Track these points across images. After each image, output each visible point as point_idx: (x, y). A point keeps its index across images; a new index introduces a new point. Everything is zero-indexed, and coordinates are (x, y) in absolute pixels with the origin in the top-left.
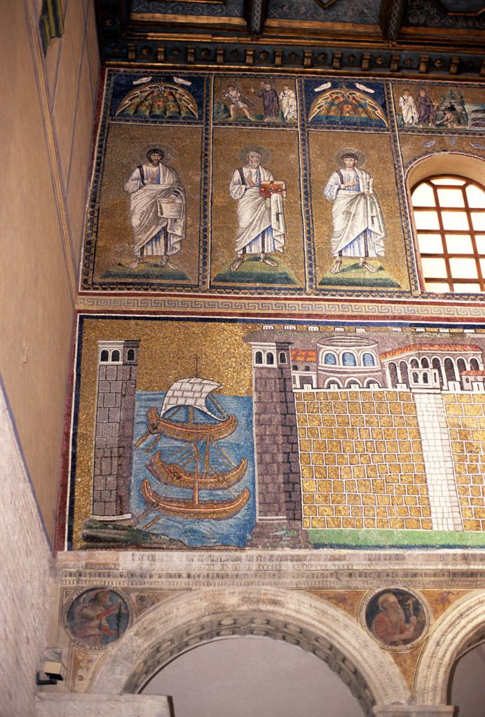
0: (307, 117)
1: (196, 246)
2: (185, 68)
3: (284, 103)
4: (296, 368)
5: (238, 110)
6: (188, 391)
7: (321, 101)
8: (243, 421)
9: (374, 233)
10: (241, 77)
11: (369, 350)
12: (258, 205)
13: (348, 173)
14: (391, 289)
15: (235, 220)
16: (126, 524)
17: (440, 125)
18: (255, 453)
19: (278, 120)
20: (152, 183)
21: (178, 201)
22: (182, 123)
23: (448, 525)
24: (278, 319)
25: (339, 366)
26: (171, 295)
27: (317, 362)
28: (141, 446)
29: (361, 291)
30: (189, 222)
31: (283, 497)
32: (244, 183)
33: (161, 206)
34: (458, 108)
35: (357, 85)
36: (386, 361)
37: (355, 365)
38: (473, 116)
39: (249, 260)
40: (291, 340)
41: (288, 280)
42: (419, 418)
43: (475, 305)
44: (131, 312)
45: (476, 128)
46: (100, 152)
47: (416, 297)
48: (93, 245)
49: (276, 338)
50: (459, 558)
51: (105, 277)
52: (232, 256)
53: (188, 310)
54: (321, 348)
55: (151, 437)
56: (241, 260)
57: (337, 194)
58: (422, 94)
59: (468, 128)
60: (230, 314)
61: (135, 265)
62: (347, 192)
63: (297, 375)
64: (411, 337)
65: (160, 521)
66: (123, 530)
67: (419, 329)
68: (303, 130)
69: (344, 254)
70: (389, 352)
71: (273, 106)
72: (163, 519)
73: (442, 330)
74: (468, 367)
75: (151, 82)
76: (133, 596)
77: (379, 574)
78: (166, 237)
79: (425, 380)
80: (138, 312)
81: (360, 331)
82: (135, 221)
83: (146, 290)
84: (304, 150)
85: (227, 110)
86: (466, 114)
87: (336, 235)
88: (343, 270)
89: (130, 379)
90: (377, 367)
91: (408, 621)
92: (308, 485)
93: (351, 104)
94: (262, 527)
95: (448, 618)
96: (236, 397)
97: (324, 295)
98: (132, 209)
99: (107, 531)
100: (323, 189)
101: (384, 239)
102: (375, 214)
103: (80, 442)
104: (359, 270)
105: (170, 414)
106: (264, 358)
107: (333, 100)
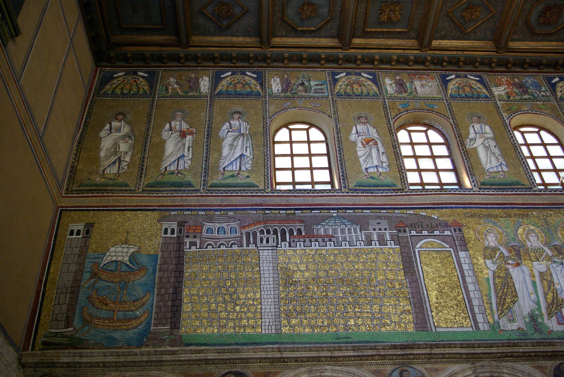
0: (214, 92)
1: (137, 167)
2: (144, 67)
3: (202, 84)
4: (188, 237)
5: (174, 89)
6: (119, 252)
7: (224, 82)
8: (151, 270)
9: (247, 156)
10: (178, 70)
11: (234, 225)
13: (235, 123)
14: (253, 189)
15: (163, 151)
16: (69, 334)
17: (294, 93)
19: (198, 94)
20: (116, 132)
21: (130, 142)
22: (139, 97)
23: (271, 329)
24: (180, 208)
25: (215, 235)
27: (201, 233)
28: (86, 286)
32: (171, 130)
34: (306, 84)
35: (247, 73)
36: (244, 231)
38: (315, 87)
39: (169, 174)
40: (187, 220)
41: (190, 185)
42: (261, 265)
43: (303, 196)
44: (92, 207)
45: (316, 95)
46: (87, 115)
47: (268, 193)
48: (75, 168)
50: (276, 350)
53: (127, 204)
54: (205, 225)
55: (92, 280)
56: (163, 174)
57: (227, 134)
58: (286, 76)
59: (311, 94)
60: (152, 206)
61: (98, 179)
62: (233, 134)
63: (187, 241)
65: (91, 332)
67: (267, 212)
68: (210, 99)
69: (226, 169)
71: (195, 86)
72: (93, 330)
74: (295, 234)
75: (124, 75)
78: (120, 163)
79: (267, 241)
80: (96, 207)
81: (230, 213)
82: (102, 154)
84: (210, 110)
85: (167, 89)
86: (311, 87)
87: (223, 158)
88: (225, 179)
89: (85, 246)
90: (238, 234)
92: (186, 307)
93: (242, 83)
94: (154, 333)
96: (149, 255)
97: (211, 193)
99: (57, 339)
100: (219, 132)
102: (248, 145)
104: (235, 178)
105: (105, 267)
106: (169, 231)
107: (231, 82)
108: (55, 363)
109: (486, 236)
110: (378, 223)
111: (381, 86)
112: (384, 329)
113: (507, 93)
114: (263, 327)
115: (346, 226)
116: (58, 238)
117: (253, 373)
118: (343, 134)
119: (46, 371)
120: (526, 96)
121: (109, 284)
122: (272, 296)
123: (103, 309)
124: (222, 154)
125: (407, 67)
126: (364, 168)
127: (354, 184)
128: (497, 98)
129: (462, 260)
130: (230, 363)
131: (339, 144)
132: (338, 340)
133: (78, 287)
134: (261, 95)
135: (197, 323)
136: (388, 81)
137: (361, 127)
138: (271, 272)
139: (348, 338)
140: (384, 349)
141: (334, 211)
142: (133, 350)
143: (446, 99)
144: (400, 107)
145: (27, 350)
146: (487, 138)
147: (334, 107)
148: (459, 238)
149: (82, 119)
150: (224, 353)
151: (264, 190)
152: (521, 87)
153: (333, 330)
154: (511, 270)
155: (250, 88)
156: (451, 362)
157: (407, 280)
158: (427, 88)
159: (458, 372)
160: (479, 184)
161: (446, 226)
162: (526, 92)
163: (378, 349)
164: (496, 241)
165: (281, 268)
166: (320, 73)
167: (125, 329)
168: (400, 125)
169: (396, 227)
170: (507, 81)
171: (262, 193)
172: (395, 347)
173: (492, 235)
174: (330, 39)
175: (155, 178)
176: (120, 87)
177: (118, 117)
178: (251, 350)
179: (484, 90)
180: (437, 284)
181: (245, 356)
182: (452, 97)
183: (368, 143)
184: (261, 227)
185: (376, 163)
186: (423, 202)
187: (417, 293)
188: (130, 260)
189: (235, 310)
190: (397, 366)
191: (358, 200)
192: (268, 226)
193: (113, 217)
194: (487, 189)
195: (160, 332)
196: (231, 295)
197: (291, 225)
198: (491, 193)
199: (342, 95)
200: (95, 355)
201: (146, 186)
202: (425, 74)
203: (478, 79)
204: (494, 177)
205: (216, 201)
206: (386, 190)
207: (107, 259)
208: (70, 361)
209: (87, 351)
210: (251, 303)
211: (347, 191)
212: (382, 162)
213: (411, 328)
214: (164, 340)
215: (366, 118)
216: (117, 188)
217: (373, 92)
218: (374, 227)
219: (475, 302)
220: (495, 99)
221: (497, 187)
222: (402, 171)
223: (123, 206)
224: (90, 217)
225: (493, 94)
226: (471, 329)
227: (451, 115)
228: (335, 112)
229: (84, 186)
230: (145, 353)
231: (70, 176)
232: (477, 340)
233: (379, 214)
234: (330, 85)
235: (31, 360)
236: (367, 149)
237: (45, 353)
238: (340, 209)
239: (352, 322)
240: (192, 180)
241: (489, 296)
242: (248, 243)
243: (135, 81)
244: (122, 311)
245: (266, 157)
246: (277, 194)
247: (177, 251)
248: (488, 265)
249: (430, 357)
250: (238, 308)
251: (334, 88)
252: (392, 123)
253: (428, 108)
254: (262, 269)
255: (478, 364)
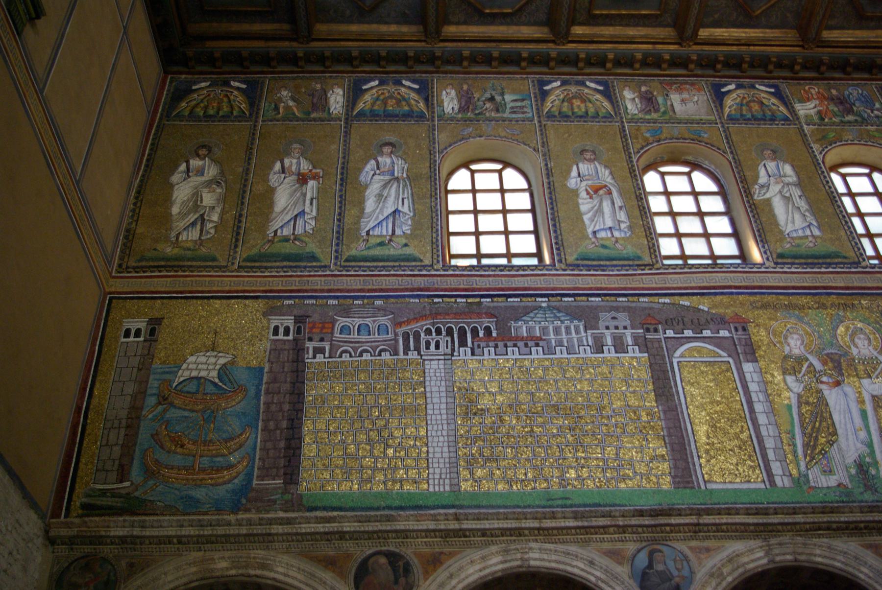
0: (352, 112)
1: (230, 230)
3: (332, 100)
4: (310, 339)
5: (287, 108)
6: (202, 364)
7: (367, 97)
8: (252, 391)
9: (403, 213)
10: (294, 79)
11: (384, 320)
12: (295, 191)
14: (414, 264)
15: (271, 205)
16: (123, 492)
17: (479, 114)
18: (260, 421)
19: (325, 115)
20: (196, 175)
21: (219, 190)
22: (233, 121)
23: (444, 485)
25: (355, 336)
26: (199, 276)
27: (332, 333)
28: (150, 416)
29: (384, 267)
30: (226, 209)
31: (282, 462)
33: (201, 196)
34: (498, 98)
35: (404, 82)
36: (400, 331)
37: (369, 335)
39: (280, 241)
40: (310, 313)
41: (313, 258)
42: (427, 383)
45: (514, 116)
46: (151, 149)
47: (437, 270)
48: (132, 232)
49: (295, 312)
50: (451, 517)
51: (140, 260)
52: (263, 239)
53: (214, 289)
54: (337, 320)
55: (160, 408)
56: (271, 242)
57: (372, 178)
58: (465, 87)
59: (505, 115)
61: (168, 250)
62: (382, 177)
63: (310, 345)
64: (428, 307)
66: (120, 497)
67: (436, 300)
68: (346, 123)
69: (371, 233)
70: (404, 322)
71: (321, 103)
73: (459, 300)
74: (481, 334)
76: (123, 563)
77: (370, 535)
78: (203, 224)
79: (437, 347)
81: (378, 303)
82: (175, 210)
83: (176, 271)
84: (345, 141)
85: (277, 108)
86: (505, 104)
87: (366, 216)
88: (369, 248)
89: (148, 354)
90: (391, 336)
91: (396, 582)
92: (309, 450)
93: (396, 99)
95: (438, 580)
96: (249, 368)
98: (174, 198)
99: (104, 499)
101: (413, 218)
103: (91, 415)
105: (181, 386)
106: (281, 330)
108: (102, 537)
109: (786, 338)
110: (614, 318)
111: (617, 102)
112: (622, 485)
113: (819, 112)
114: (431, 482)
115: (562, 322)
116: (107, 342)
117: (415, 554)
118: (556, 178)
119: (88, 549)
120: (850, 118)
121: (186, 414)
122: (445, 433)
123: (176, 453)
124: (364, 209)
125: (659, 72)
126: (590, 231)
127: (575, 256)
128: (803, 121)
129: (748, 377)
130: (379, 538)
131: (550, 193)
132: (550, 503)
133: (138, 418)
134: (426, 116)
135: (326, 475)
136: (628, 94)
137: (586, 166)
138: (443, 394)
139: (566, 499)
140: (623, 516)
141: (544, 299)
142: (225, 517)
143: (722, 123)
144: (648, 135)
145: (59, 516)
146: (788, 184)
147: (542, 134)
148: (743, 343)
149: (143, 155)
150: (369, 521)
151: (432, 266)
152: (841, 103)
153: (543, 486)
154: (826, 393)
155: (409, 105)
156: (730, 538)
157: (660, 408)
158: (690, 105)
159: (742, 554)
160: (775, 256)
161: (721, 322)
162: (850, 111)
163: (614, 516)
164: (802, 347)
165: (460, 389)
166: (520, 82)
167: (212, 485)
168: (647, 163)
169: (642, 326)
170: (819, 92)
171: (429, 271)
172: (641, 513)
173: (795, 336)
174: (533, 28)
175: (258, 247)
176: (202, 105)
177: (200, 152)
178: (411, 518)
179: (782, 108)
180: (708, 414)
181: (402, 528)
182: (731, 118)
183: (596, 191)
184: (426, 324)
185: (609, 223)
186: (684, 285)
187: (675, 427)
188: (220, 377)
189: (385, 455)
190: (644, 544)
191: (581, 282)
192: (438, 323)
193: (192, 308)
194: (787, 264)
195: (267, 489)
196: (379, 432)
197: (474, 322)
198: (793, 270)
199: (555, 116)
200: (165, 524)
201: (245, 260)
202: (686, 83)
203: (773, 90)
204: (798, 246)
205: (355, 283)
206: (625, 266)
207: (183, 374)
208: (125, 533)
209: (151, 518)
210: (412, 443)
211: (563, 267)
212: (619, 221)
213: (666, 483)
214: (275, 501)
215: (594, 152)
216: (198, 263)
217: (604, 111)
218: (607, 324)
219: (769, 443)
220: (800, 123)
221: (803, 261)
222: (652, 236)
223: (209, 292)
224: (157, 308)
225: (796, 115)
226: (762, 486)
227: (730, 148)
228: (543, 143)
229: (147, 260)
230: (244, 522)
231: (124, 244)
232: (773, 503)
233: (615, 304)
234: (536, 101)
235: (64, 532)
236: (596, 201)
237: (86, 522)
238: (553, 295)
239: (572, 474)
240: (317, 251)
241: (791, 433)
242: (407, 349)
243: (227, 96)
244: (207, 456)
245: (434, 215)
246: (451, 273)
247: (293, 362)
248: (790, 385)
249: (696, 530)
250: (390, 452)
251: (542, 105)
252: (635, 160)
253: (692, 137)
254: (428, 389)
255: (773, 541)
